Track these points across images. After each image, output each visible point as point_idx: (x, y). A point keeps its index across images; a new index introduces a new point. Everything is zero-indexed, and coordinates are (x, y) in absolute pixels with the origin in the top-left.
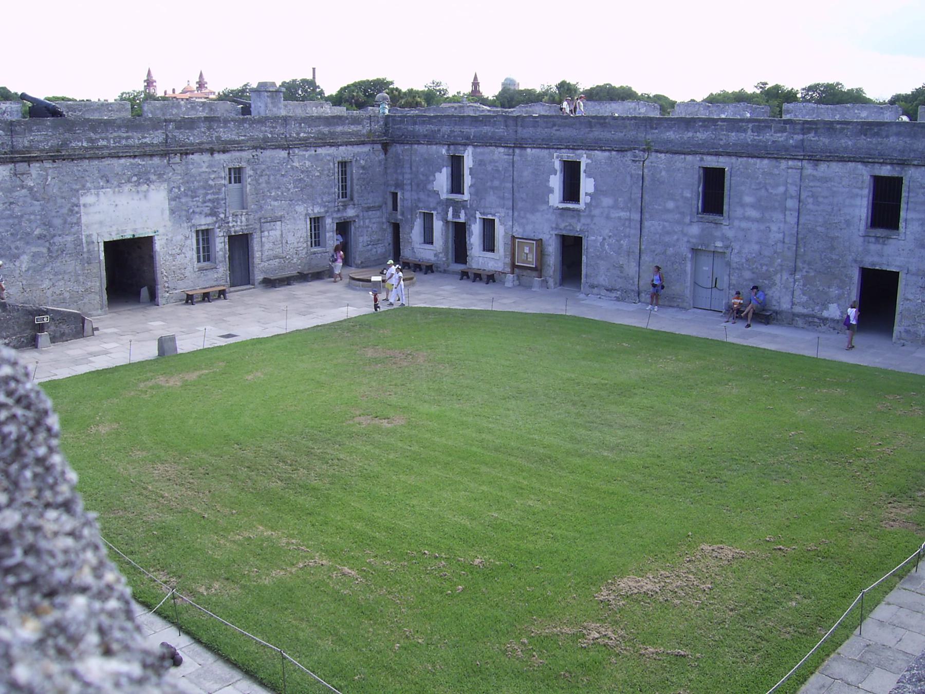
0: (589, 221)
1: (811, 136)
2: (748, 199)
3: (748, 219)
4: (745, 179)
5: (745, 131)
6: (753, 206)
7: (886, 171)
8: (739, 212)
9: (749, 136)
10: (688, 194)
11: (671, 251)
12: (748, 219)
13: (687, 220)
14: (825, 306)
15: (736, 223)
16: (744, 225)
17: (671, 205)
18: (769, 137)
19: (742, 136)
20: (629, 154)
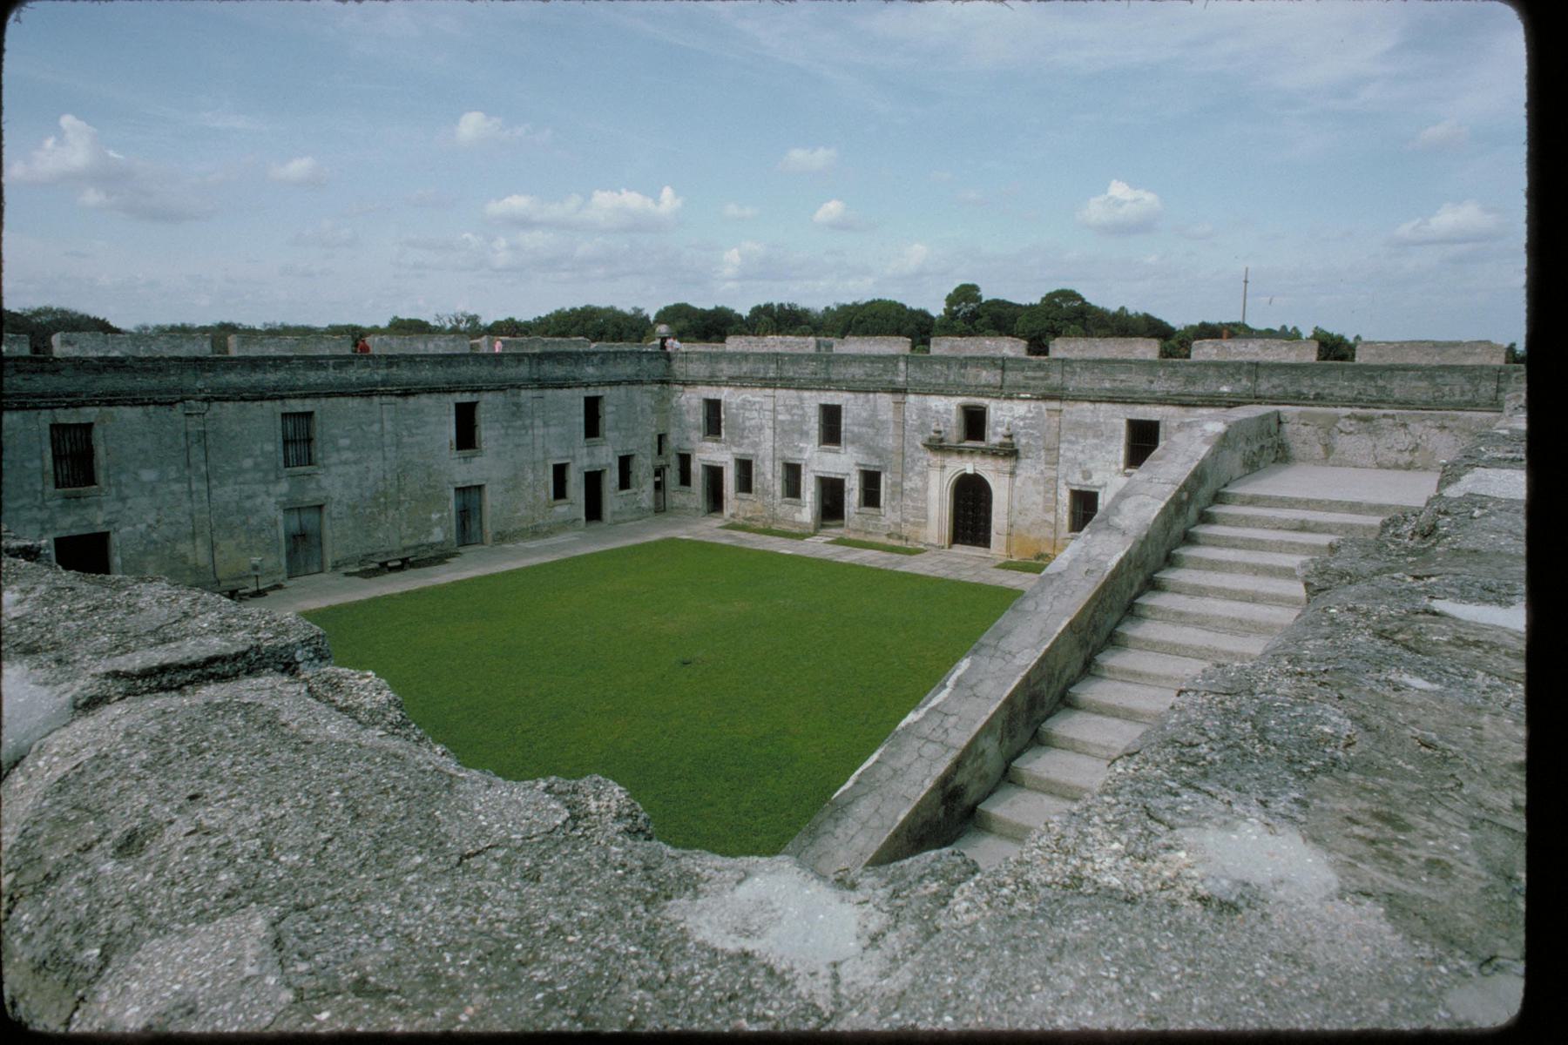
0: (119, 505)
1: (394, 369)
2: (344, 442)
3: (345, 463)
4: (338, 420)
5: (325, 368)
6: (348, 448)
7: (466, 398)
8: (334, 458)
9: (330, 375)
10: (269, 447)
11: (254, 521)
12: (345, 463)
13: (272, 477)
14: (429, 533)
15: (333, 469)
16: (341, 469)
17: (248, 463)
18: (353, 374)
19: (323, 374)
20: (178, 406)
